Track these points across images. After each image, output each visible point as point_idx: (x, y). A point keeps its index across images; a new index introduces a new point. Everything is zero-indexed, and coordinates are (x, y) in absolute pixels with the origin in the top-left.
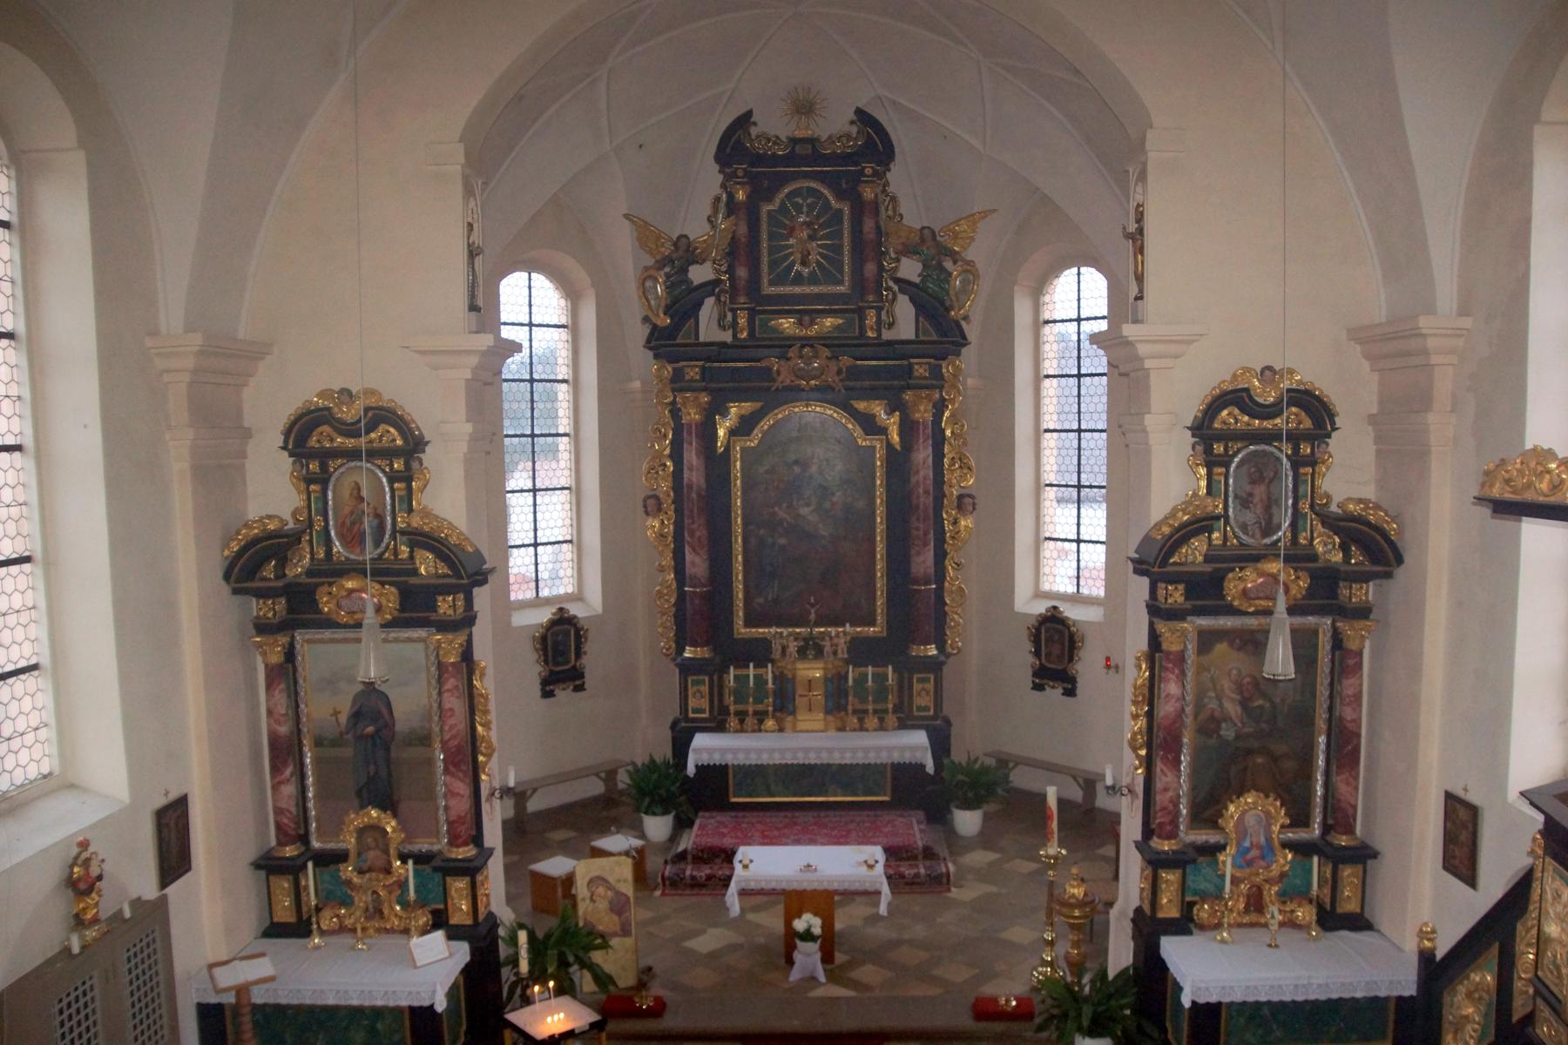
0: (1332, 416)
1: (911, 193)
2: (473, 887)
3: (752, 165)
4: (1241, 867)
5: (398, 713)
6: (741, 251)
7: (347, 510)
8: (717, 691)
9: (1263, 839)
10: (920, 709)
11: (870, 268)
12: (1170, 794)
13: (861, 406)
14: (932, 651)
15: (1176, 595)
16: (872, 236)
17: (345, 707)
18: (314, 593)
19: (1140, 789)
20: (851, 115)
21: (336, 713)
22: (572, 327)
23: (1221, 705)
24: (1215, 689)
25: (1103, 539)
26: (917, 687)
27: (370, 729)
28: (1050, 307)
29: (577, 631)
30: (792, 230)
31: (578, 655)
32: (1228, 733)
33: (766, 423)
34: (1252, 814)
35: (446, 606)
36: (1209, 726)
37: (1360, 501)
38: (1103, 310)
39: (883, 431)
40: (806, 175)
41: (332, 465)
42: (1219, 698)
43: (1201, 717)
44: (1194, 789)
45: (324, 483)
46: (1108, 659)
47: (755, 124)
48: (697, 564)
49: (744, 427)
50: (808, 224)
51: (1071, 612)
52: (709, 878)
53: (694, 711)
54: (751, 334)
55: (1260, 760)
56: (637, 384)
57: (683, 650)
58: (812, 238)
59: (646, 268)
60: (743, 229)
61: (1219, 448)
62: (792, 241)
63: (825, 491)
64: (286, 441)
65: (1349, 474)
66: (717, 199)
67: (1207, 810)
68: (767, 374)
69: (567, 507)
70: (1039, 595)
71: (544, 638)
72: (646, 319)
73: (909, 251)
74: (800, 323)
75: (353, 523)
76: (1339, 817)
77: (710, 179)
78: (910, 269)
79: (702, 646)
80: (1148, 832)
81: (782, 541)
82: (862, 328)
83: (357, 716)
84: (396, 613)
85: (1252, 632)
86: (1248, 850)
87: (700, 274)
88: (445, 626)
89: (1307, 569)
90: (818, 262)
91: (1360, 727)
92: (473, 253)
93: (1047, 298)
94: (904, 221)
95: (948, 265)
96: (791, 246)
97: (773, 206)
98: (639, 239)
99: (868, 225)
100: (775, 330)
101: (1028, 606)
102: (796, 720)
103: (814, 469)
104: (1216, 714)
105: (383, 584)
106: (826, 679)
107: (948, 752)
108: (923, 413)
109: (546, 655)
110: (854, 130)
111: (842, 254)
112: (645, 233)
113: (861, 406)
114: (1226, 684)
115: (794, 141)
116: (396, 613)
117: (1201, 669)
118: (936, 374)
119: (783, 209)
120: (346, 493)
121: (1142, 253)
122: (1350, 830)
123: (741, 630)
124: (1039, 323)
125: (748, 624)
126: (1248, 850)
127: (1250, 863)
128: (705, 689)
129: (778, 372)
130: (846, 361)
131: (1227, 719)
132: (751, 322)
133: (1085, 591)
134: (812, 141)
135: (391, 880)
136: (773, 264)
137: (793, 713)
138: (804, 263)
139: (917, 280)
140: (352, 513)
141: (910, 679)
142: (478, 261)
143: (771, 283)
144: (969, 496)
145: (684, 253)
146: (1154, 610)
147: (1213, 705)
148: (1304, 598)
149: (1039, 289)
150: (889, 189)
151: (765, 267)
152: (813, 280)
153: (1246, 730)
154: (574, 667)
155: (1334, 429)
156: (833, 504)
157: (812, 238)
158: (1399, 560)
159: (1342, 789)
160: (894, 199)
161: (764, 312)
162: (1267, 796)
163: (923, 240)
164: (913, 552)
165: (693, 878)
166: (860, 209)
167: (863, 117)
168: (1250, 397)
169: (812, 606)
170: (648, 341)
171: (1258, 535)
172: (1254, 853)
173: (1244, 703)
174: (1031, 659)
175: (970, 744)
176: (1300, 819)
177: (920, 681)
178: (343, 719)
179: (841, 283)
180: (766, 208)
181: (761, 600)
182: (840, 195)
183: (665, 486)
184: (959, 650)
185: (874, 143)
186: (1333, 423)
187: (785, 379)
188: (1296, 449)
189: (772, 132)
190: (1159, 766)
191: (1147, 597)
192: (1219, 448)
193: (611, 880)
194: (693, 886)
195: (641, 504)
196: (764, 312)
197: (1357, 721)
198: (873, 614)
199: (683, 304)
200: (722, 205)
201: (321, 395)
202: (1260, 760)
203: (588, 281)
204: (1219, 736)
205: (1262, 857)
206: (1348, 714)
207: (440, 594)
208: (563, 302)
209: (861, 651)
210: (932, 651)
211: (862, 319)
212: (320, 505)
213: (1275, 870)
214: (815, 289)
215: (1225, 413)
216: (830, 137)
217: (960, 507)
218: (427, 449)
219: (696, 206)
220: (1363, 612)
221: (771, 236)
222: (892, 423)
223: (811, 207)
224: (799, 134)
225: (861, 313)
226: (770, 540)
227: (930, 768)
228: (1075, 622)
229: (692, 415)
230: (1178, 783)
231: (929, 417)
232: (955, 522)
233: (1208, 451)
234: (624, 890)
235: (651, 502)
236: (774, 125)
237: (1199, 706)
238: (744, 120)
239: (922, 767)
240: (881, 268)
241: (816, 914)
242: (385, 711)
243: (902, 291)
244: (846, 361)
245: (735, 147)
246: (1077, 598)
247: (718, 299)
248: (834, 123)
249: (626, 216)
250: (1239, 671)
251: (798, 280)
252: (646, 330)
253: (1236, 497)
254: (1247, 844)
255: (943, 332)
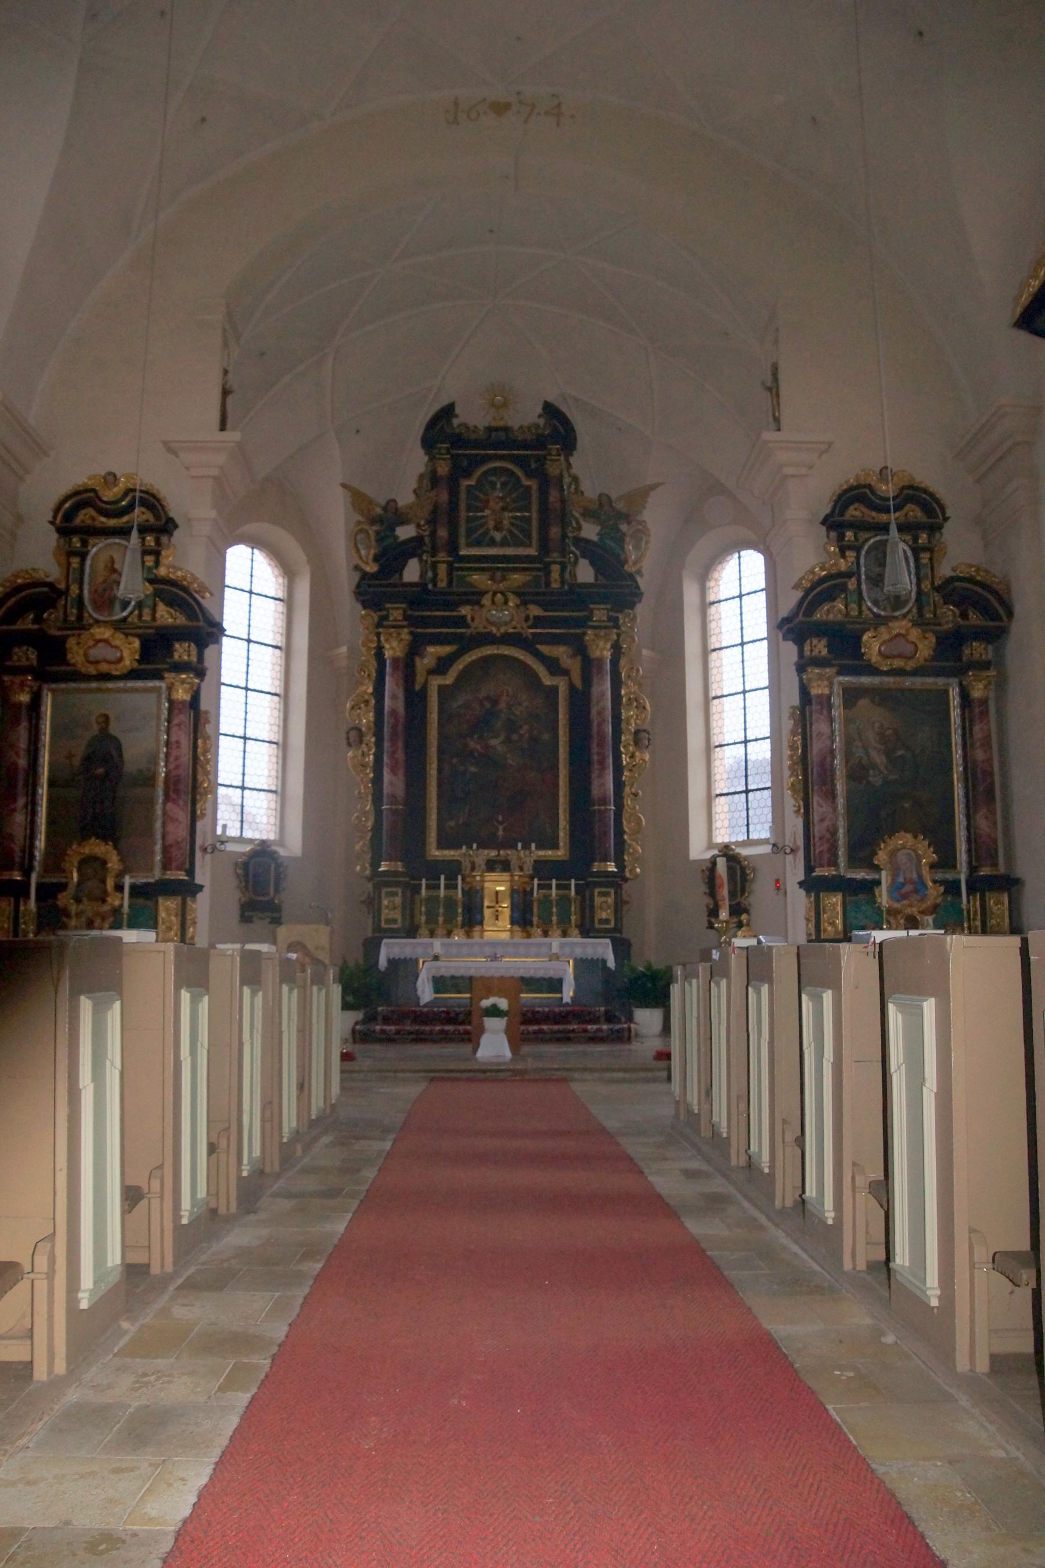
0: (943, 509)
1: (590, 472)
2: (183, 913)
3: (453, 445)
4: (898, 901)
5: (127, 755)
6: (442, 516)
7: (100, 579)
8: (409, 908)
9: (915, 876)
10: (601, 921)
11: (555, 531)
12: (826, 824)
13: (545, 649)
14: (612, 867)
15: (820, 647)
16: (558, 505)
17: (80, 750)
18: (65, 642)
19: (800, 842)
20: (539, 410)
21: (70, 756)
22: (288, 602)
23: (867, 754)
24: (861, 740)
25: (769, 785)
26: (598, 900)
27: (101, 771)
28: (715, 590)
29: (278, 866)
30: (488, 501)
31: (277, 890)
32: (875, 779)
33: (459, 666)
34: (905, 852)
35: (182, 651)
36: (857, 773)
37: (971, 566)
38: (765, 682)
39: (566, 672)
40: (502, 458)
41: (92, 541)
42: (865, 748)
43: (849, 765)
44: (849, 831)
45: (83, 556)
46: (777, 881)
47: (457, 416)
48: (393, 783)
49: (442, 666)
50: (502, 499)
51: (738, 850)
52: (398, 1032)
53: (388, 921)
54: (450, 583)
55: (907, 805)
56: (344, 649)
57: (379, 866)
58: (504, 509)
59: (359, 523)
60: (444, 497)
61: (849, 535)
62: (487, 512)
63: (512, 726)
64: (55, 517)
65: (959, 551)
66: (421, 477)
67: (862, 851)
68: (461, 622)
69: (274, 760)
70: (711, 845)
71: (246, 865)
72: (357, 568)
73: (588, 514)
74: (492, 579)
75: (105, 590)
76: (982, 850)
77: (417, 461)
78: (590, 531)
79: (396, 860)
80: (809, 869)
81: (473, 769)
82: (548, 584)
83: (89, 759)
84: (136, 665)
85: (889, 690)
86: (903, 885)
87: (405, 532)
88: (180, 667)
89: (934, 632)
90: (510, 532)
91: (991, 766)
92: (226, 392)
93: (712, 584)
94: (586, 494)
95: (624, 527)
96: (486, 517)
97: (472, 482)
98: (353, 505)
99: (554, 495)
100: (471, 585)
101: (698, 850)
102: (483, 931)
103: (502, 705)
104: (865, 761)
105: (127, 635)
106: (513, 892)
107: (628, 956)
108: (602, 650)
109: (247, 882)
110: (542, 422)
111: (530, 525)
112: (358, 499)
113: (545, 649)
114: (871, 736)
115: (490, 429)
116: (136, 665)
117: (848, 721)
118: (615, 623)
119: (479, 485)
120: (101, 565)
121: (778, 396)
122: (992, 859)
123: (435, 853)
124: (705, 606)
125: (440, 846)
126: (903, 885)
127: (904, 897)
128: (398, 900)
129: (473, 619)
130: (535, 611)
131: (873, 766)
132: (450, 573)
133: (754, 836)
134: (506, 429)
135: (106, 908)
136: (470, 532)
137: (481, 923)
138: (497, 528)
139: (595, 538)
140: (105, 581)
141: (592, 900)
142: (230, 399)
143: (469, 545)
144: (645, 731)
145: (390, 517)
146: (801, 669)
147: (859, 753)
148: (933, 658)
149: (704, 576)
150: (574, 471)
151: (462, 531)
152: (504, 543)
153: (892, 777)
154: (272, 901)
155: (946, 519)
156: (521, 736)
157: (504, 509)
158: (1010, 614)
159: (982, 824)
160: (575, 479)
161: (462, 569)
162: (915, 837)
163: (601, 505)
164: (594, 775)
165: (383, 1031)
166: (545, 482)
167: (550, 411)
168: (873, 492)
169: (501, 823)
170: (358, 586)
171: (889, 610)
172: (908, 888)
173: (888, 753)
174: (707, 900)
175: (649, 954)
176: (946, 860)
177: (601, 894)
178: (77, 761)
179: (530, 545)
180: (465, 483)
181: (452, 823)
182: (530, 475)
183: (367, 718)
184: (637, 876)
185: (558, 430)
186: (943, 513)
187: (478, 626)
188: (915, 539)
189: (471, 424)
190: (816, 799)
191: (794, 657)
192: (849, 535)
193: (310, 946)
194: (381, 1041)
195: (344, 736)
196: (462, 569)
197: (989, 761)
198: (556, 837)
199: (392, 557)
200: (426, 483)
201: (89, 478)
202: (907, 805)
203: (304, 558)
204: (868, 782)
205: (916, 891)
206: (980, 755)
207: (178, 640)
208: (281, 580)
209: (543, 870)
210: (612, 867)
211: (548, 573)
212: (77, 576)
213: (929, 903)
214: (510, 551)
215: (852, 508)
216: (521, 427)
217: (637, 743)
218: (176, 533)
219: (405, 476)
220: (986, 665)
221: (469, 509)
222: (573, 665)
223: (504, 485)
224: (494, 424)
225: (547, 569)
226: (462, 768)
227: (611, 964)
228: (746, 858)
229: (394, 649)
230: (835, 816)
231: (607, 654)
232: (632, 756)
233: (841, 537)
234: (321, 958)
235: (353, 734)
236: (473, 416)
237: (848, 756)
238: (448, 412)
239: (604, 962)
240: (564, 536)
241: (500, 997)
242: (114, 753)
243: (584, 557)
244: (535, 611)
245: (441, 431)
246: (748, 843)
247: (421, 560)
248: (524, 415)
249: (344, 485)
250: (882, 726)
251: (492, 543)
252: (356, 577)
253: (867, 578)
254: (901, 880)
255: (619, 590)
